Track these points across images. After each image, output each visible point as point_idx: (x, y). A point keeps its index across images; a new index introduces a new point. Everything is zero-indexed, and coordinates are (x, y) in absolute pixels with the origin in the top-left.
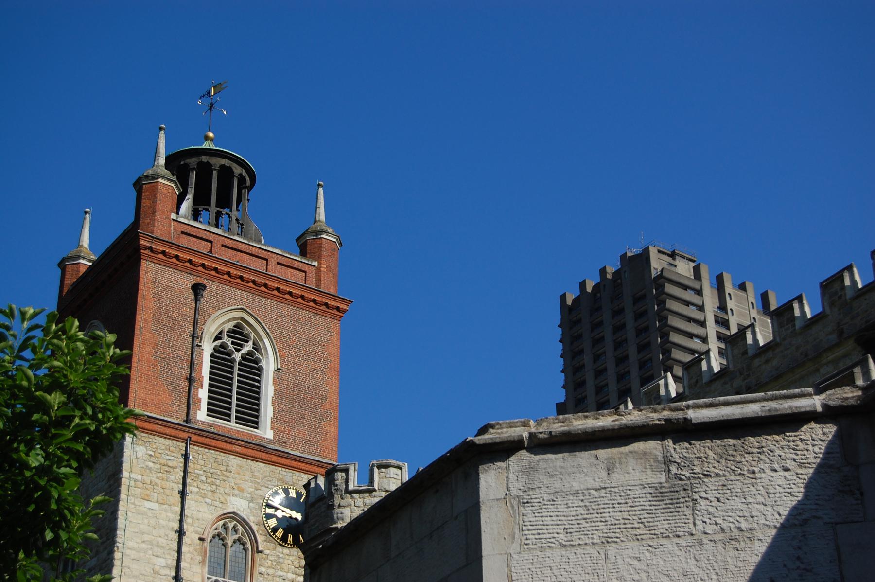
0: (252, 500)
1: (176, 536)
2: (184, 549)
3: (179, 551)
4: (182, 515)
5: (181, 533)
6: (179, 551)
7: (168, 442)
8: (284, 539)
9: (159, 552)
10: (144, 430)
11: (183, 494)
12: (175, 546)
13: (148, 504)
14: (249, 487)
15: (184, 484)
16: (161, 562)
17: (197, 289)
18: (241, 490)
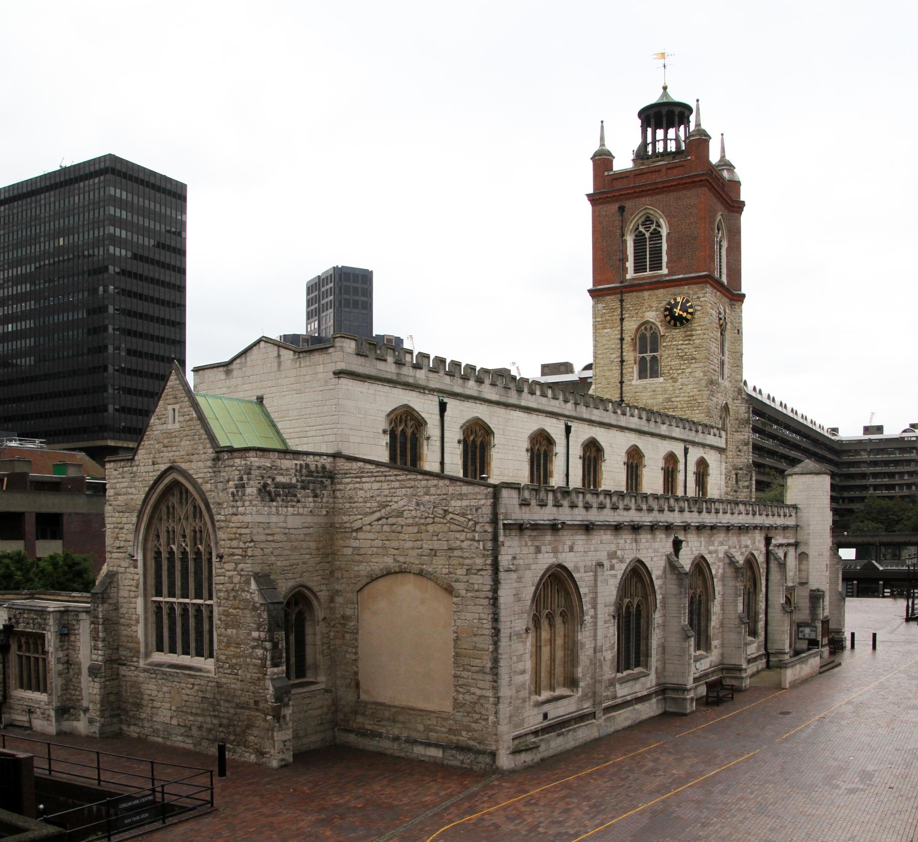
0: (657, 311)
1: (619, 341)
2: (624, 346)
3: (622, 348)
4: (622, 330)
5: (622, 339)
6: (622, 348)
7: (612, 297)
8: (675, 325)
9: (612, 351)
10: (599, 296)
11: (622, 320)
12: (619, 346)
13: (605, 331)
14: (655, 304)
15: (622, 314)
16: (614, 356)
18: (651, 307)
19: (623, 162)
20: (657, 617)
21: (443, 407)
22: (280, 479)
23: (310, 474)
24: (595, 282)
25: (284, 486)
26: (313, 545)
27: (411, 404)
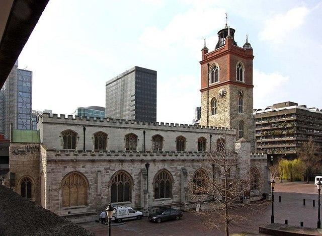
5: (208, 103)
11: (208, 98)
17: (208, 64)
19: (211, 48)
20: (135, 187)
21: (84, 129)
22: (19, 150)
23: (31, 148)
24: (202, 87)
25: (21, 151)
26: (31, 165)
27: (71, 129)
